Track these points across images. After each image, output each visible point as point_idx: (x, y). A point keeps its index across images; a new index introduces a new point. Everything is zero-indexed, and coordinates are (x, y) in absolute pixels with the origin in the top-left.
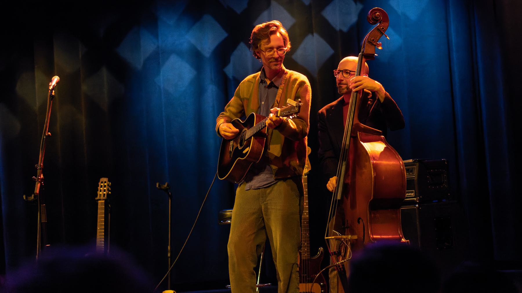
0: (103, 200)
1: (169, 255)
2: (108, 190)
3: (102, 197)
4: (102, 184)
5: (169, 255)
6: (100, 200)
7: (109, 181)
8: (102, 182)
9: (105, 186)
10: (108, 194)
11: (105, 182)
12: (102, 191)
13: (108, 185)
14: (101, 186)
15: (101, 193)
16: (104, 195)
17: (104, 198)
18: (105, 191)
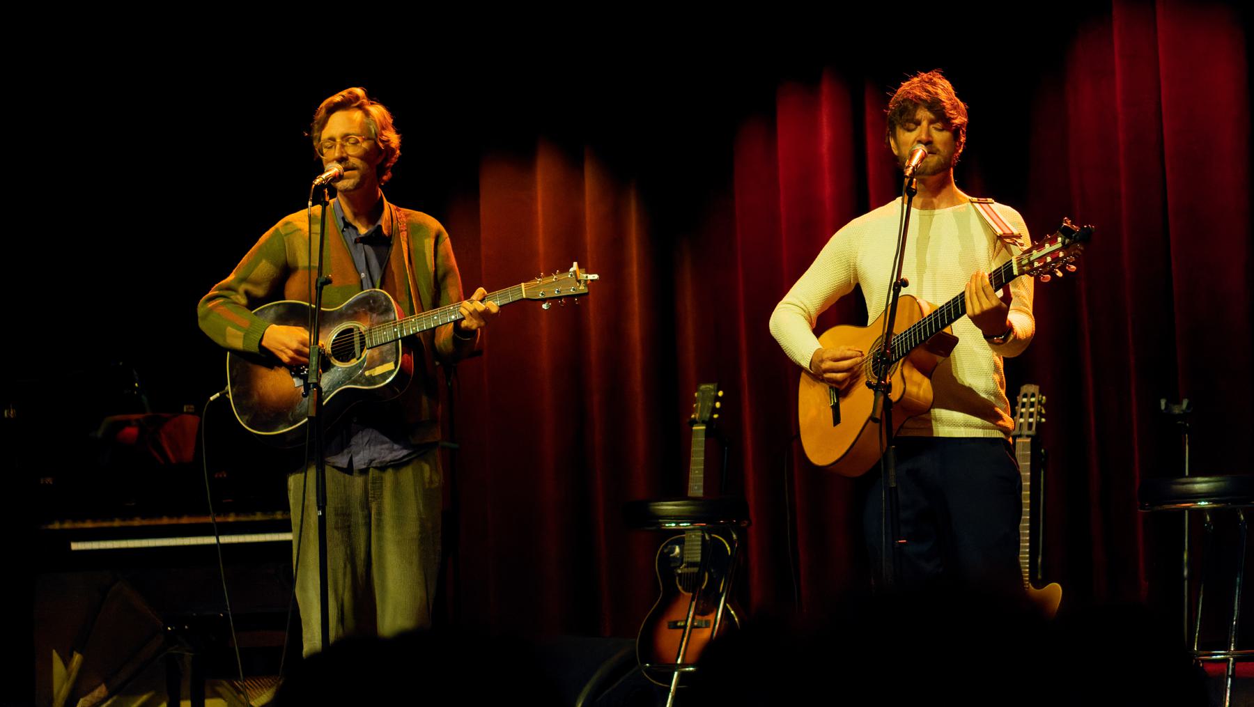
0: (1028, 436)
1: (1186, 573)
2: (1039, 413)
3: (1025, 431)
4: (1025, 400)
5: (1186, 573)
6: (1020, 436)
7: (1042, 392)
8: (1025, 396)
9: (1032, 405)
10: (1039, 424)
11: (1033, 395)
12: (1028, 405)
13: (1040, 402)
14: (1024, 405)
15: (1022, 420)
16: (1030, 425)
17: (1030, 433)
18: (1031, 415)
